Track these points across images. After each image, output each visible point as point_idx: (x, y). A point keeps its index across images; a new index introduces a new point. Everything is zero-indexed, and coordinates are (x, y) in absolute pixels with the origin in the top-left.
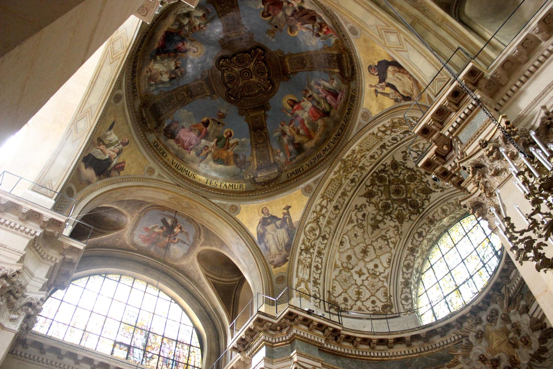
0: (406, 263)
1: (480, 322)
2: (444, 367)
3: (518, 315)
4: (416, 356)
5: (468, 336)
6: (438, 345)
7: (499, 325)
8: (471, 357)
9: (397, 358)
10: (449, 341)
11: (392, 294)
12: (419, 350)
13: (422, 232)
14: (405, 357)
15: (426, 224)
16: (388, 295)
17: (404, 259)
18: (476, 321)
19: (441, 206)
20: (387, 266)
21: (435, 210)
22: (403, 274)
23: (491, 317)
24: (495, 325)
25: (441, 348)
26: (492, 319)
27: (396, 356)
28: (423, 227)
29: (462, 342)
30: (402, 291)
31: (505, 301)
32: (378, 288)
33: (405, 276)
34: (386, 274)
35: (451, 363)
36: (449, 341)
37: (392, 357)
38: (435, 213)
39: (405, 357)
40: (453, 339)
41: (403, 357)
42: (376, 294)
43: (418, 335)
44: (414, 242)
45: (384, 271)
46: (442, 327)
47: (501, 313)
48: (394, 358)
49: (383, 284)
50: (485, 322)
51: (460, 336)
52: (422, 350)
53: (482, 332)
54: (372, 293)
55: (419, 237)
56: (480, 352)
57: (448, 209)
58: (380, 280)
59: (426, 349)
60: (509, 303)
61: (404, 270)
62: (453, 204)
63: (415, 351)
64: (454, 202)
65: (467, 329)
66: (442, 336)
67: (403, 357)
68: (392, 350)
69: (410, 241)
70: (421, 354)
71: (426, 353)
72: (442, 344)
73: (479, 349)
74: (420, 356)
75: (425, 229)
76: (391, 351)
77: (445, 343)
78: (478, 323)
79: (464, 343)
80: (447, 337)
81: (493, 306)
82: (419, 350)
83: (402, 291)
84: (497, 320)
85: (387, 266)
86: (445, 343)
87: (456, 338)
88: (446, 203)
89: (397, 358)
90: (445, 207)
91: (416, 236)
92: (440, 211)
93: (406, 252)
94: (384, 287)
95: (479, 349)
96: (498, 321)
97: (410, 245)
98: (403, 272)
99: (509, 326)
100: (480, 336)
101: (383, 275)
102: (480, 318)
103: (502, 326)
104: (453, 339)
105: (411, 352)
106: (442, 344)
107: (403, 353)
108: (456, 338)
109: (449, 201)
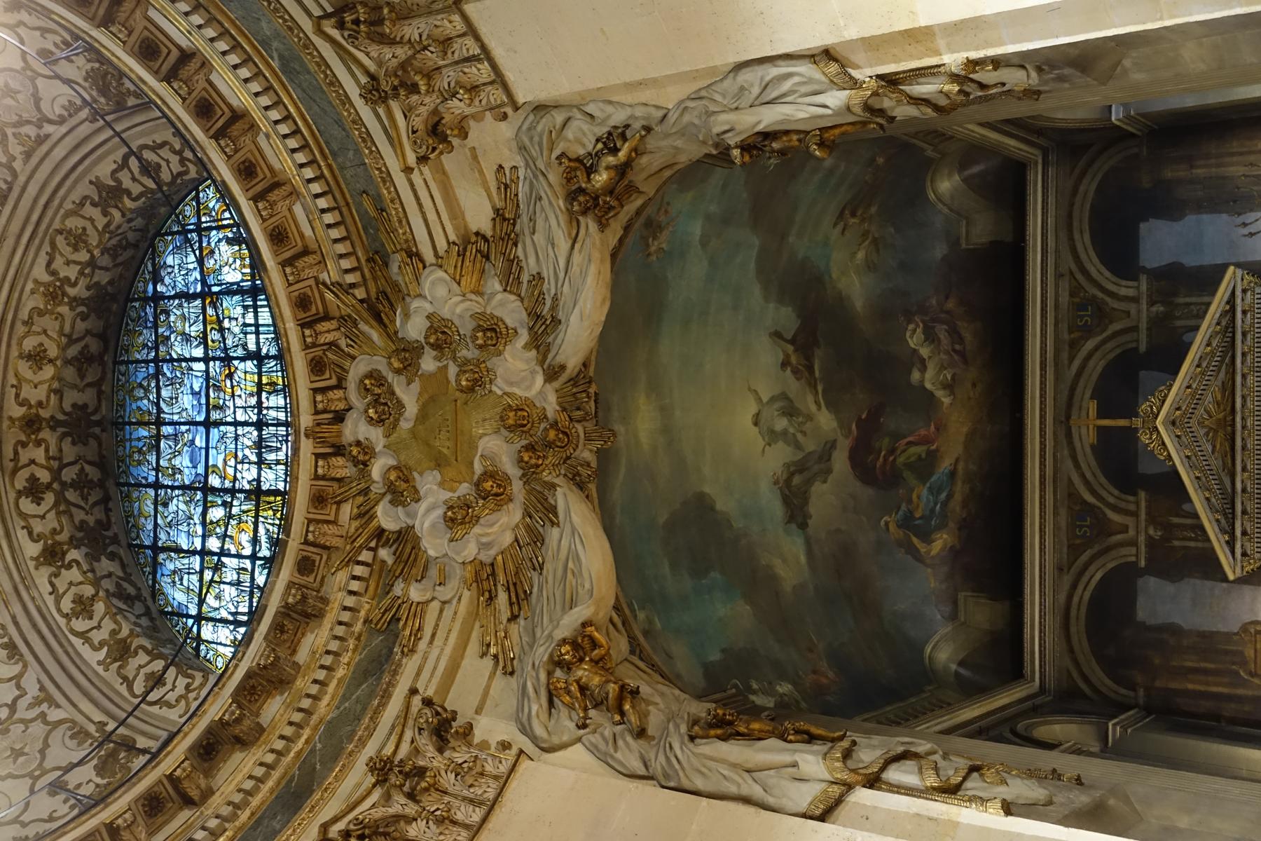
0: (67, 605)
1: (363, 456)
2: (399, 665)
3: (415, 304)
4: (307, 742)
5: (380, 532)
6: (334, 645)
7: (409, 396)
8: (431, 553)
9: (255, 801)
10: (350, 601)
11: (98, 717)
12: (297, 717)
13: (33, 479)
14: (276, 775)
15: (24, 445)
16: (92, 729)
17: (50, 601)
18: (356, 462)
19: (15, 353)
20: (17, 669)
21: (12, 380)
22: (88, 640)
23: (376, 402)
24: (400, 405)
25: (351, 643)
26: (384, 409)
27: (246, 803)
28: (24, 459)
29: (384, 562)
30: (125, 679)
31: (363, 327)
32: (39, 745)
33: (97, 636)
34: (33, 690)
35: (407, 632)
36: (350, 601)
37: (234, 817)
38: (18, 387)
39: (276, 775)
40: (355, 585)
41: (271, 783)
42: (48, 764)
43: (249, 675)
44: (38, 527)
45: (18, 687)
46: (290, 585)
47: (380, 364)
48: (244, 816)
49: (46, 723)
50: (376, 436)
51: (366, 556)
52: (306, 703)
53: (396, 468)
54: (30, 775)
55: (38, 501)
56: (439, 512)
57: (43, 338)
58: (26, 722)
59: (314, 689)
60: (378, 317)
61: (80, 625)
62: (41, 313)
63: (288, 731)
64: (37, 301)
65: (360, 516)
66: (319, 615)
67: (271, 783)
68: (216, 800)
69: (22, 535)
70: (315, 719)
71: (326, 700)
72: (340, 630)
73: (428, 511)
74: (315, 728)
75: (33, 462)
76: (216, 802)
77: (345, 617)
78: (365, 465)
79: (390, 561)
80: (338, 598)
81: (357, 370)
82: (297, 717)
83: (125, 679)
84: (393, 393)
85: (17, 669)
86: (345, 617)
87: (359, 570)
88: (20, 329)
89: (255, 801)
90: (29, 344)
91: (27, 505)
92: (24, 368)
93: (42, 577)
94: (61, 722)
95: (428, 511)
96: (398, 391)
97: (32, 549)
98: (82, 635)
99: (428, 363)
100: (401, 490)
101: (23, 703)
102: (358, 443)
103: (416, 386)
104: (355, 585)
105: (279, 745)
106: (340, 630)
107: (259, 772)
108: (359, 570)
109: (24, 314)
